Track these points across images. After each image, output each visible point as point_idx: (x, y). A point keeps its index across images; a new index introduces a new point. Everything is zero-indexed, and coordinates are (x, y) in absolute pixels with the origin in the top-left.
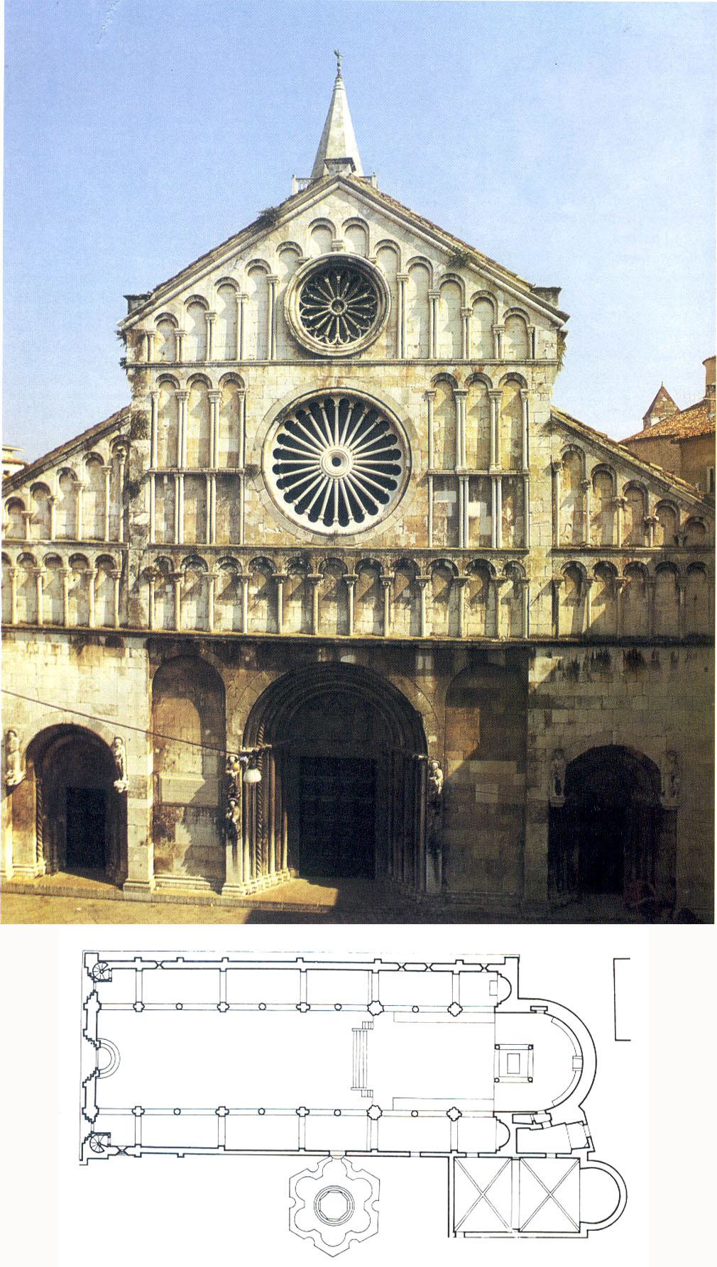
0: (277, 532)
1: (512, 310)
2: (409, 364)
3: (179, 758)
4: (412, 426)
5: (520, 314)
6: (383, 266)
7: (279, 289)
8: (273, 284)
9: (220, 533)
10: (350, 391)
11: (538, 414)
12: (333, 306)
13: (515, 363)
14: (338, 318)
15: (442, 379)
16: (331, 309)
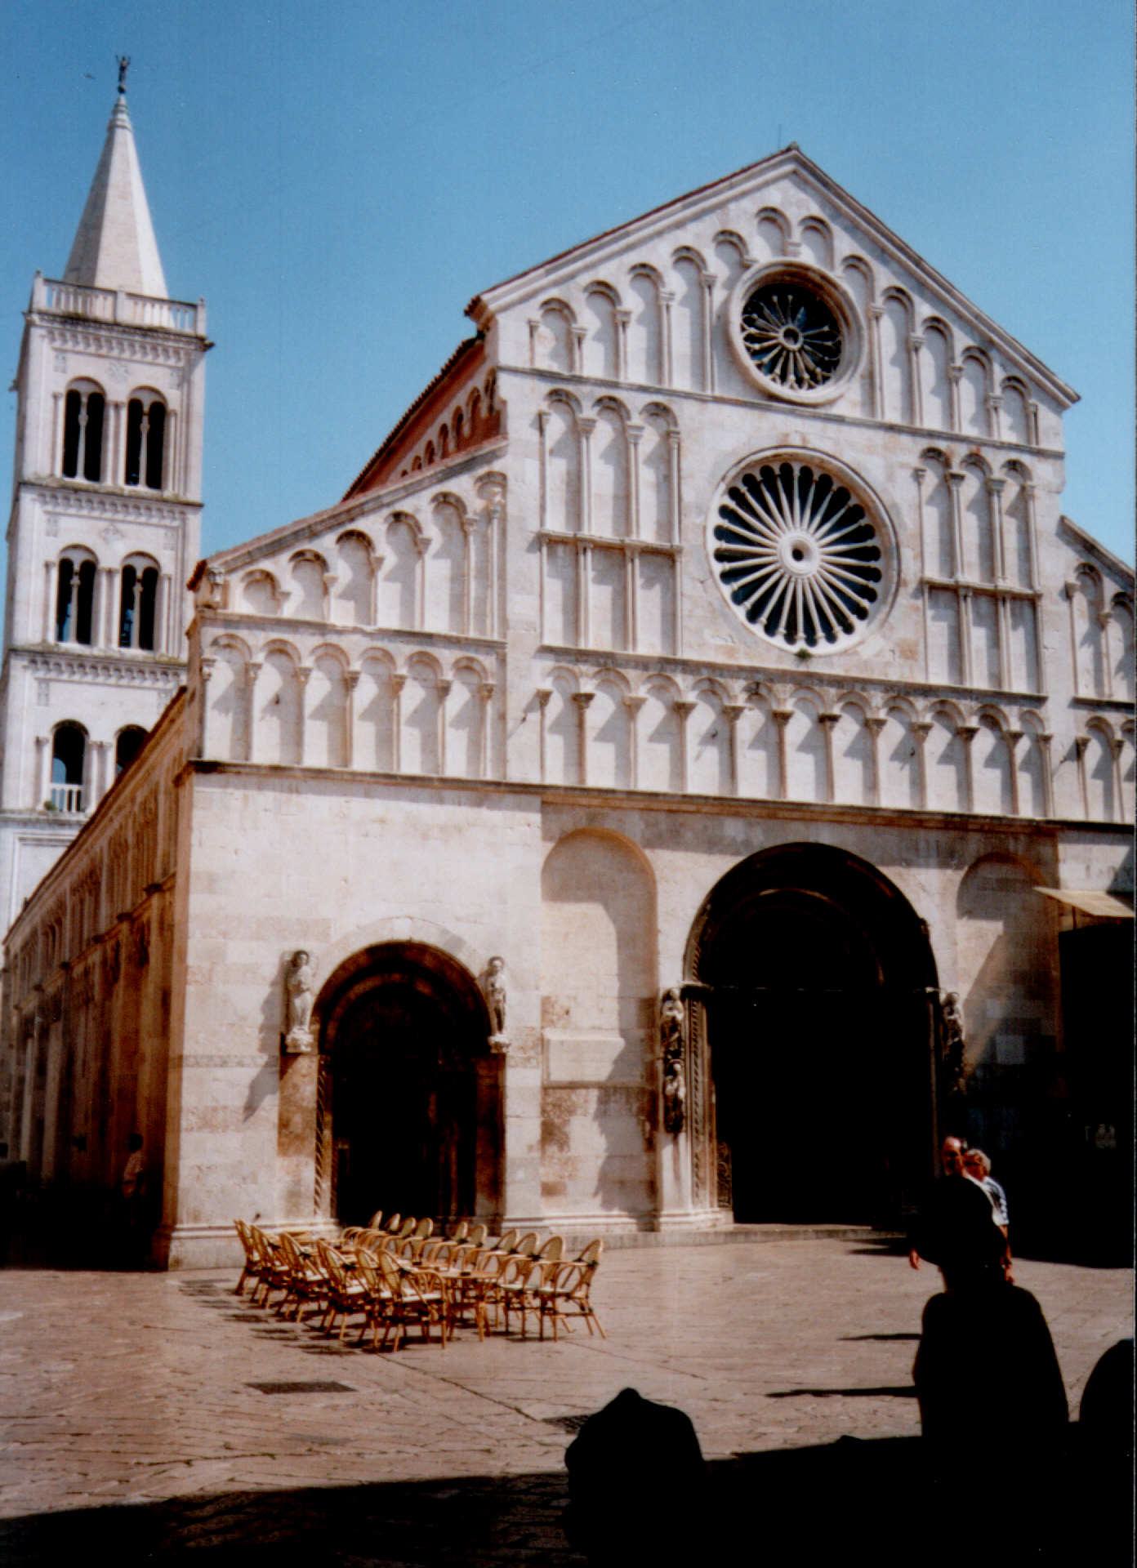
0: (730, 644)
2: (891, 428)
4: (898, 513)
7: (719, 295)
9: (649, 643)
11: (1044, 520)
14: (791, 355)
15: (932, 454)
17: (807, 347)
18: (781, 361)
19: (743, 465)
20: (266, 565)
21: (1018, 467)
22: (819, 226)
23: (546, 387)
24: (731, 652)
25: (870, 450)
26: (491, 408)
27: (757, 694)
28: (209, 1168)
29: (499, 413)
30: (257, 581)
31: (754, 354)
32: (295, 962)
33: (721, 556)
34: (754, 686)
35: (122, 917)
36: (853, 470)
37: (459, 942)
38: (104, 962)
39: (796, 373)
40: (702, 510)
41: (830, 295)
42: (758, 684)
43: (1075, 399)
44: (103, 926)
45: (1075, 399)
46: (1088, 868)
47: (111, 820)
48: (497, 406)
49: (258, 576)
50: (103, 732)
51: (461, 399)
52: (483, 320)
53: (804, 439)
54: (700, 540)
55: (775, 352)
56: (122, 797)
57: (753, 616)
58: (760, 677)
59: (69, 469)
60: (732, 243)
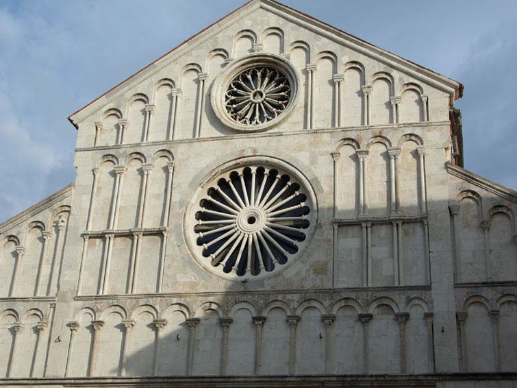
2: (316, 132)
4: (318, 182)
6: (296, 60)
8: (203, 81)
9: (144, 284)
10: (264, 158)
12: (255, 95)
14: (257, 105)
24: (193, 285)
25: (300, 148)
40: (184, 204)
41: (283, 67)
53: (255, 151)
55: (262, 106)
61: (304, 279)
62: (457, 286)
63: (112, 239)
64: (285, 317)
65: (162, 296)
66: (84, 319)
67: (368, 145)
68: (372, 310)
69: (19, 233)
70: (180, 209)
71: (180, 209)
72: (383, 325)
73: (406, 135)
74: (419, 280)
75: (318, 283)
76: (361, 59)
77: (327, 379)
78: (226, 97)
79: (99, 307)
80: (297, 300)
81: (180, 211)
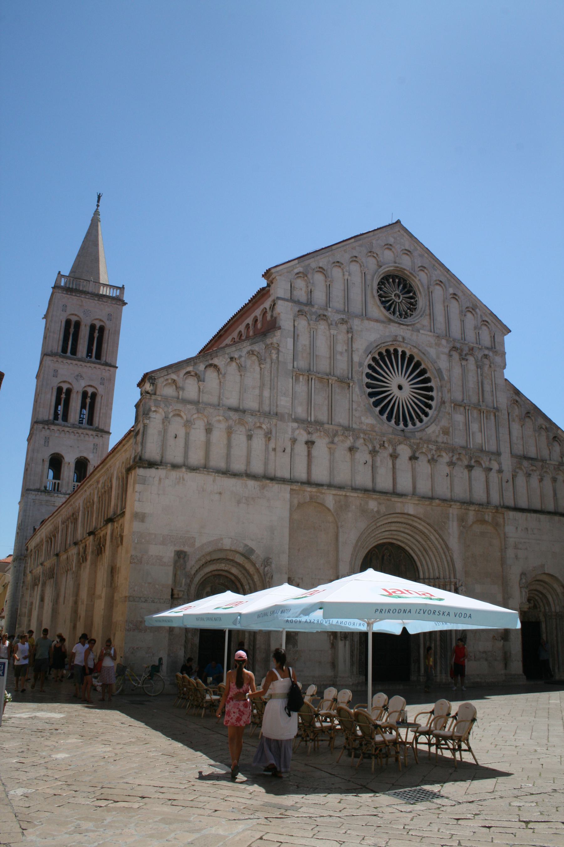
1: (483, 321)
3: (302, 581)
4: (441, 372)
5: (487, 324)
13: (487, 348)
14: (397, 304)
15: (454, 348)
16: (393, 297)
17: (403, 301)
18: (393, 306)
19: (378, 347)
20: (174, 376)
21: (488, 357)
22: (409, 253)
23: (297, 309)
24: (373, 426)
26: (272, 316)
27: (384, 446)
28: (137, 648)
29: (276, 318)
30: (169, 384)
31: (383, 302)
32: (180, 555)
33: (368, 386)
34: (382, 442)
35: (90, 533)
36: (423, 353)
37: (252, 551)
38: (78, 554)
39: (399, 311)
42: (384, 442)
43: (510, 331)
44: (79, 536)
45: (510, 331)
46: (517, 528)
47: (86, 491)
48: (274, 315)
49: (170, 381)
50: (70, 459)
51: (258, 312)
52: (271, 279)
53: (403, 338)
54: (360, 378)
56: (93, 480)
57: (382, 412)
58: (385, 439)
59: (64, 350)
60: (374, 257)
61: (437, 436)
62: (513, 455)
63: (313, 378)
64: (426, 459)
65: (353, 430)
66: (303, 437)
67: (466, 355)
68: (473, 463)
69: (240, 357)
70: (360, 368)
71: (360, 368)
72: (478, 473)
73: (484, 355)
74: (493, 448)
75: (445, 441)
76: (460, 294)
77: (453, 503)
78: (377, 290)
79: (310, 431)
80: (435, 449)
81: (360, 370)
